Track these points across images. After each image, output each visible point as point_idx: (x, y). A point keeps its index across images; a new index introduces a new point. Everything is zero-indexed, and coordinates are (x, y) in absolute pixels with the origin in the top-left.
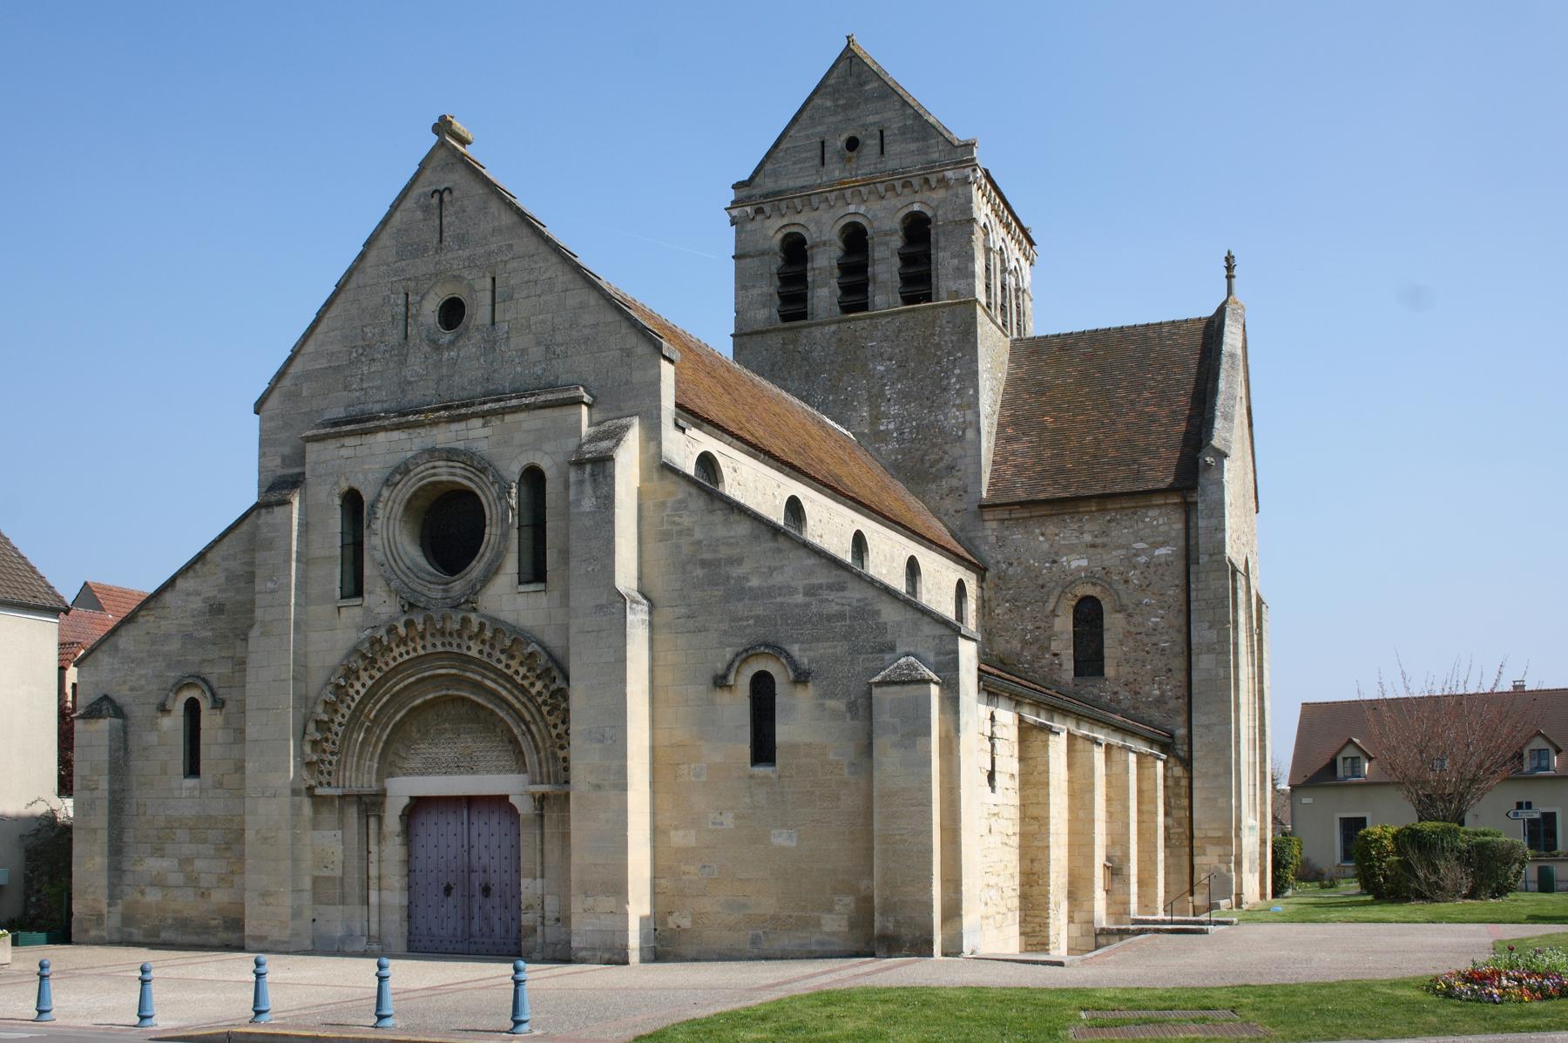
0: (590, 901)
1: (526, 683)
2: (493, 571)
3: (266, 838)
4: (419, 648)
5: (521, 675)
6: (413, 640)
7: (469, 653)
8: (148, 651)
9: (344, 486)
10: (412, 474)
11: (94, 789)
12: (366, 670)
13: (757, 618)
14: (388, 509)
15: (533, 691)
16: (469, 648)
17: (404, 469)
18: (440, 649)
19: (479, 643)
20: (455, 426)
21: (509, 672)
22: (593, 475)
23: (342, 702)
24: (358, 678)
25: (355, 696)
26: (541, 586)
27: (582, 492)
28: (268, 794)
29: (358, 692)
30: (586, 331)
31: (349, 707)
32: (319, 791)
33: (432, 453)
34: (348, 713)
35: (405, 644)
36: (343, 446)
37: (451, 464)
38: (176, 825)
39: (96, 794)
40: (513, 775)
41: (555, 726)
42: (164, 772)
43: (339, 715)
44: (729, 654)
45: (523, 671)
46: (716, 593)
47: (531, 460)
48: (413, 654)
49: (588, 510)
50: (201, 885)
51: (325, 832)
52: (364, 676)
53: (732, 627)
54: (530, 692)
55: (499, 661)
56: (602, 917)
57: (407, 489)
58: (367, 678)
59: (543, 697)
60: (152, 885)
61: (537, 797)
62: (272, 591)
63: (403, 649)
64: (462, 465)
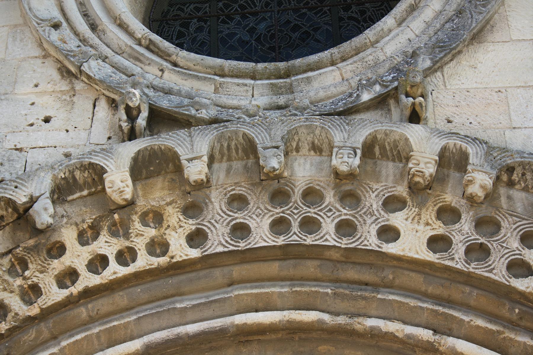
7: (391, 248)
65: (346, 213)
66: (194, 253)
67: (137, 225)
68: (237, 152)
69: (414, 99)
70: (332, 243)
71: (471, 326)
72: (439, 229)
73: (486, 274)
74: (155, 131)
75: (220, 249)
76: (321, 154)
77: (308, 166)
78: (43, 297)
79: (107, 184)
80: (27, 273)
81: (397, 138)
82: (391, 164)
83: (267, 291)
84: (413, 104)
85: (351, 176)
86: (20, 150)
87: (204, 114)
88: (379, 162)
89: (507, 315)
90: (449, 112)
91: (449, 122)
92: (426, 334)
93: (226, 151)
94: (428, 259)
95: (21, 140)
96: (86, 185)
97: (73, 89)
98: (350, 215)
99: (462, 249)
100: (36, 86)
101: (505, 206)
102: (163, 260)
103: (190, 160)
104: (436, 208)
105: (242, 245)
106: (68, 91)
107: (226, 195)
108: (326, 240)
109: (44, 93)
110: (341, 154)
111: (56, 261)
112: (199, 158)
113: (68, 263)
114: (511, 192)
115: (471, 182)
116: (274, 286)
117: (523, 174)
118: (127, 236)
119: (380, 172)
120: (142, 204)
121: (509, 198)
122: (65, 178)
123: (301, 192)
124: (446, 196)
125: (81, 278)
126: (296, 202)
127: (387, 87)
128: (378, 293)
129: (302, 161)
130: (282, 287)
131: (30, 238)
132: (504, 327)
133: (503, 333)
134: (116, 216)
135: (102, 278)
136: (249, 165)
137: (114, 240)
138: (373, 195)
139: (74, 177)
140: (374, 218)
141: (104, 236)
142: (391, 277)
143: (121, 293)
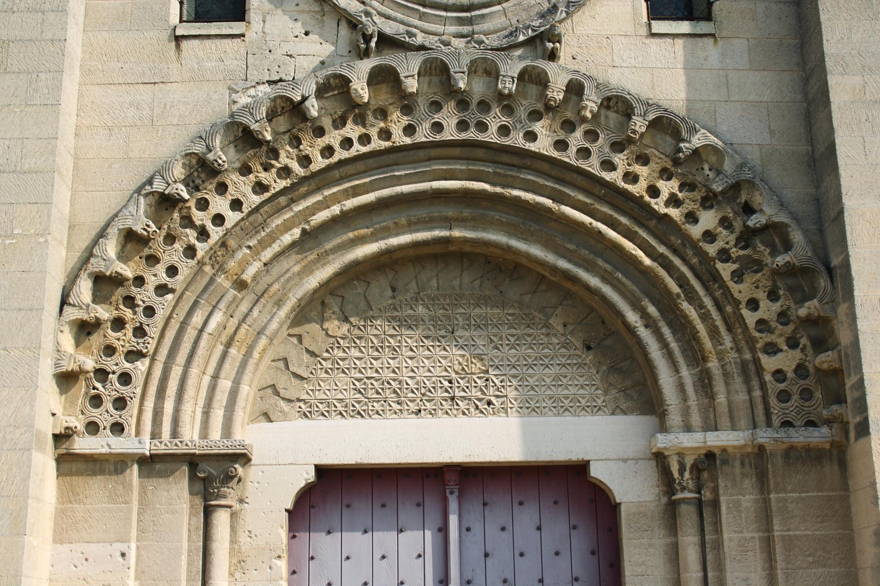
1: (674, 213)
5: (665, 195)
6: (383, 114)
7: (532, 147)
12: (246, 170)
15: (695, 231)
16: (531, 136)
18: (450, 133)
19: (557, 125)
21: (638, 189)
23: (170, 239)
24: (222, 189)
25: (210, 227)
26: (704, 27)
29: (219, 219)
31: (190, 252)
32: (83, 444)
35: (361, 120)
40: (596, 419)
41: (753, 304)
43: (161, 269)
45: (667, 187)
48: (378, 144)
51: (94, 550)
54: (687, 238)
55: (609, 166)
58: (248, 190)
59: (719, 244)
61: (689, 461)
63: (352, 131)
65: (505, 120)
66: (408, 141)
67: (370, 118)
68: (436, 71)
69: (554, 44)
70: (495, 141)
71: (575, 200)
72: (561, 136)
73: (588, 169)
74: (381, 49)
75: (424, 139)
76: (490, 77)
77: (481, 84)
78: (313, 164)
79: (352, 91)
80: (301, 147)
81: (540, 71)
82: (534, 87)
83: (452, 167)
84: (553, 48)
85: (510, 95)
86: (291, 56)
88: (527, 84)
89: (597, 193)
90: (575, 51)
91: (574, 58)
92: (548, 202)
93: (428, 69)
94: (553, 156)
96: (336, 87)
97: (323, 10)
98: (507, 122)
99: (574, 149)
100: (297, 5)
101: (603, 122)
102: (388, 144)
103: (406, 77)
104: (561, 121)
105: (438, 138)
106: (320, 12)
107: (428, 100)
108: (492, 138)
109: (303, 11)
110: (505, 81)
111: (319, 139)
112: (413, 76)
113: (327, 142)
114: (608, 113)
115: (585, 108)
116: (456, 164)
117: (617, 103)
118: (364, 126)
119: (527, 92)
120: (374, 104)
121: (606, 117)
122: (324, 83)
123: (476, 102)
124: (568, 113)
125: (336, 153)
126: (473, 110)
127: (536, 31)
128: (521, 173)
129: (477, 80)
130: (462, 165)
131: (301, 123)
132: (595, 200)
133: (594, 205)
134: (357, 111)
135: (349, 154)
136: (443, 80)
137: (356, 128)
138: (522, 109)
139: (329, 82)
140: (522, 125)
141: (350, 125)
142: (529, 163)
143: (360, 163)
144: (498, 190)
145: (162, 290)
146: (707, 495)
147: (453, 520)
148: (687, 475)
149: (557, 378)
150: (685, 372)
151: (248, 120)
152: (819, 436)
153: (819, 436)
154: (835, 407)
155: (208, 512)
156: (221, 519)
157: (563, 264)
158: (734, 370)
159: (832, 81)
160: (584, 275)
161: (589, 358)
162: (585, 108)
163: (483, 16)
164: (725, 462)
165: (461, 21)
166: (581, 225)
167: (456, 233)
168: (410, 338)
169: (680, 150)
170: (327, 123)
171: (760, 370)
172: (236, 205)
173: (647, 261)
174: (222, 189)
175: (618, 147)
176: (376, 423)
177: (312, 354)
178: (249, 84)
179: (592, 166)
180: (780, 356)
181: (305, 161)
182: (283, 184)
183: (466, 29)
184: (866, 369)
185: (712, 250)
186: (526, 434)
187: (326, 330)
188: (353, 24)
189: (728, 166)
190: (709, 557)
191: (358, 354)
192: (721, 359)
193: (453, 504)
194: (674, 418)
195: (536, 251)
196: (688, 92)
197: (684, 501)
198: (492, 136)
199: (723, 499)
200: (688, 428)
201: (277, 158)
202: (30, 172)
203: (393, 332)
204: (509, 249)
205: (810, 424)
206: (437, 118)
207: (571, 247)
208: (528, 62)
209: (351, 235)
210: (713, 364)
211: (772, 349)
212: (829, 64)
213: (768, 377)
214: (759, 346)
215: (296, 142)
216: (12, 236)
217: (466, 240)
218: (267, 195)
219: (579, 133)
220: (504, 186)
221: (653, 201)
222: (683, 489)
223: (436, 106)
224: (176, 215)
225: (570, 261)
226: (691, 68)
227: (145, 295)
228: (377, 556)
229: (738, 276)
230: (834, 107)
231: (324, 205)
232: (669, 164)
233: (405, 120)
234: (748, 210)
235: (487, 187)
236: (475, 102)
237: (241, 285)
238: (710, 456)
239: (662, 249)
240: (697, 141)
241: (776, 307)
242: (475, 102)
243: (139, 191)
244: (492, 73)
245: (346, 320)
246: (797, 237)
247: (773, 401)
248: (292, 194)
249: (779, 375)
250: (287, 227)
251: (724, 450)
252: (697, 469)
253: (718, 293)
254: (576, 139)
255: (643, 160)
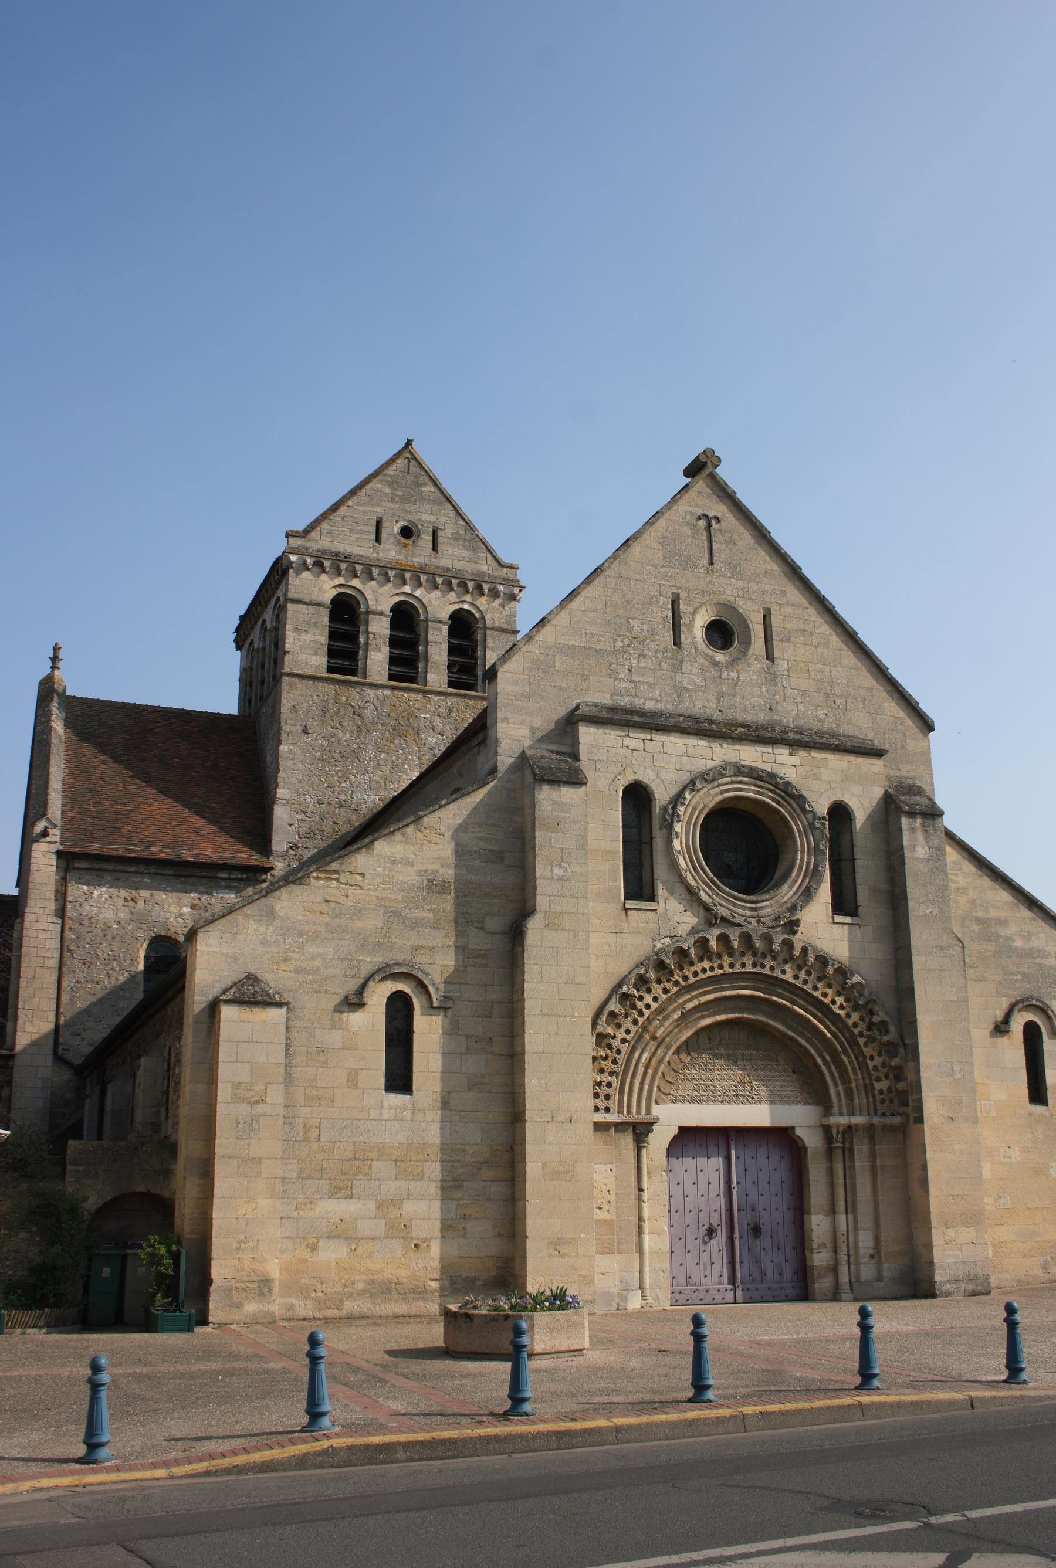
0: (950, 1233)
1: (842, 1013)
2: (808, 894)
3: (558, 1173)
4: (726, 965)
5: (838, 1004)
7: (784, 977)
8: (327, 925)
9: (629, 778)
10: (716, 783)
11: (257, 1102)
13: (1024, 975)
14: (688, 814)
15: (850, 1022)
16: (784, 972)
17: (707, 777)
18: (749, 969)
19: (795, 968)
20: (760, 748)
21: (827, 1000)
22: (923, 825)
23: (626, 1016)
24: (649, 991)
25: (644, 1010)
26: (856, 920)
27: (916, 839)
28: (561, 1118)
29: (648, 1006)
30: (863, 692)
31: (635, 1022)
33: (739, 770)
34: (633, 1029)
35: (710, 959)
36: (628, 736)
37: (759, 783)
38: (373, 1154)
39: (259, 1109)
40: (795, 1107)
41: (872, 1058)
42: (353, 1081)
43: (622, 1030)
44: (1005, 1005)
45: (840, 1000)
46: (989, 948)
47: (839, 797)
49: (922, 857)
50: (414, 1235)
52: (657, 989)
53: (1005, 980)
54: (846, 1025)
55: (815, 988)
56: (964, 1247)
57: (709, 798)
58: (660, 991)
60: (330, 1237)
61: (841, 1129)
62: (561, 879)
63: (706, 964)
64: (772, 787)
65: (772, 963)
66: (730, 971)
67: (714, 959)
87: (737, 921)
92: (788, 1004)
95: (677, 918)
102: (721, 972)
105: (744, 970)
144: (767, 996)
145: (624, 1041)
146: (847, 1145)
147: (733, 1153)
148: (839, 1136)
149: (781, 1087)
150: (841, 1088)
151: (664, 958)
152: (896, 1120)
153: (896, 1120)
154: (904, 1108)
155: (639, 1149)
156: (644, 1152)
157: (791, 1033)
158: (862, 1088)
159: (914, 958)
160: (799, 1039)
161: (795, 1077)
162: (809, 960)
163: (762, 907)
164: (856, 1130)
165: (752, 909)
166: (801, 1016)
167: (746, 1016)
168: (719, 1063)
169: (847, 984)
170: (695, 960)
171: (873, 1088)
172: (655, 999)
173: (829, 1035)
174: (649, 991)
175: (819, 979)
176: (704, 1106)
177: (675, 1071)
178: (661, 937)
179: (808, 988)
180: (882, 1082)
181: (685, 978)
182: (676, 989)
183: (755, 913)
184: (923, 1094)
185: (856, 1031)
186: (772, 1113)
187: (681, 1059)
188: (707, 909)
189: (866, 993)
190: (848, 1173)
191: (695, 1072)
192: (856, 1080)
193: (733, 1146)
194: (836, 1110)
195: (779, 1026)
196: (850, 953)
197: (838, 1147)
198: (767, 971)
199: (855, 1148)
200: (841, 1115)
201: (673, 975)
202: (579, 984)
203: (709, 1061)
204: (768, 1024)
205: (893, 1115)
206: (744, 960)
207: (795, 1025)
208: (785, 936)
209: (700, 1014)
210: (853, 1085)
211: (878, 1080)
212: (913, 950)
213: (876, 1092)
214: (873, 1077)
215: (681, 969)
216: (574, 1017)
217: (749, 1019)
218: (669, 995)
219: (803, 972)
220: (769, 995)
221: (833, 1007)
222: (837, 1142)
223: (743, 954)
224: (628, 1003)
225: (793, 1031)
226: (851, 940)
227: (616, 1043)
228: (699, 1170)
229: (866, 1045)
230: (914, 972)
231: (691, 1000)
232: (840, 989)
233: (730, 960)
234: (871, 1013)
235: (762, 994)
236: (760, 953)
237: (654, 1038)
238: (850, 1127)
239: (834, 1029)
240: (856, 979)
241: (881, 1059)
242: (760, 953)
243: (614, 991)
244: (768, 939)
245: (689, 1054)
246: (892, 1028)
247: (878, 1104)
248: (678, 994)
249: (881, 1092)
250: (674, 1011)
251: (856, 1125)
252: (844, 1133)
253: (856, 1052)
254: (802, 975)
255: (830, 986)
